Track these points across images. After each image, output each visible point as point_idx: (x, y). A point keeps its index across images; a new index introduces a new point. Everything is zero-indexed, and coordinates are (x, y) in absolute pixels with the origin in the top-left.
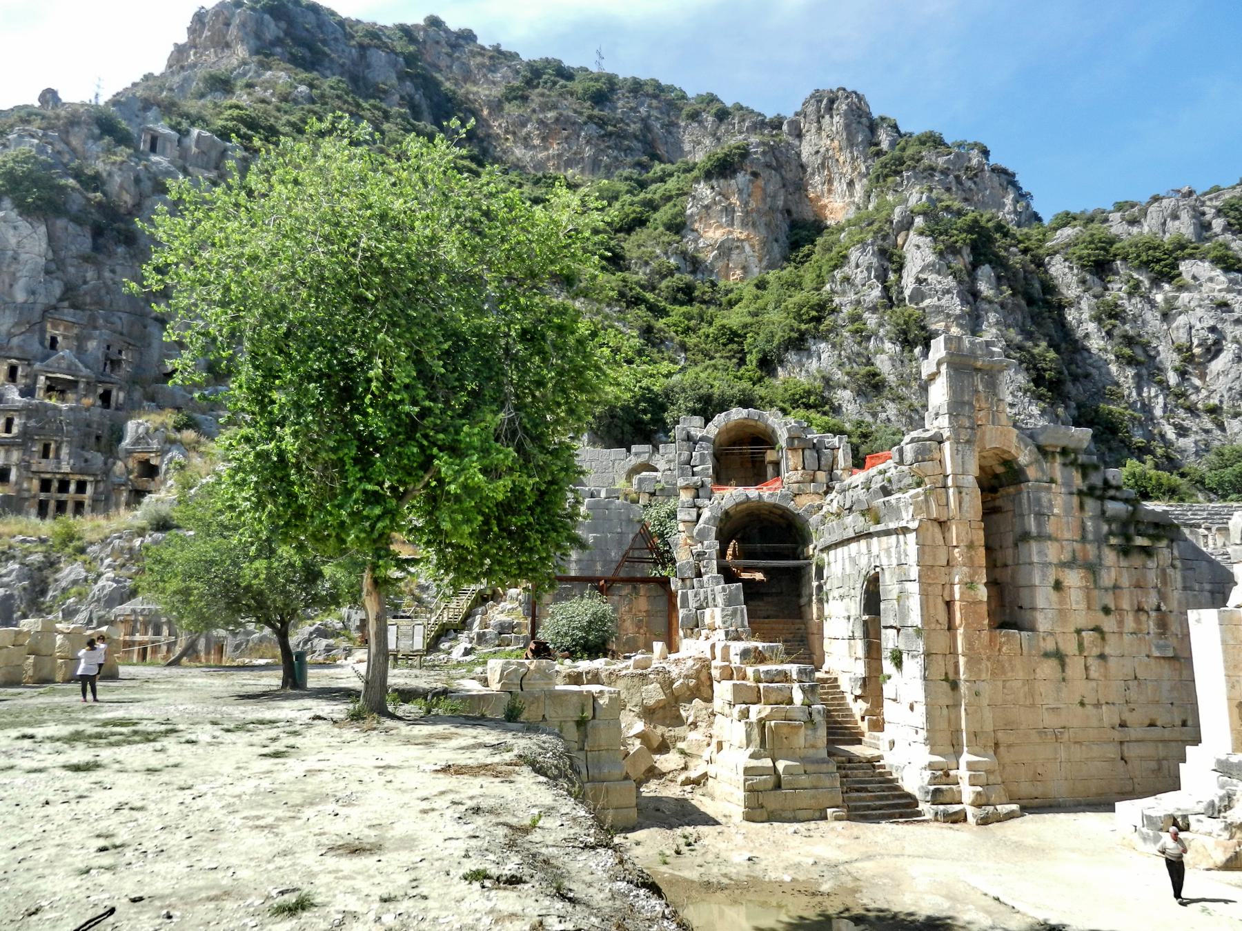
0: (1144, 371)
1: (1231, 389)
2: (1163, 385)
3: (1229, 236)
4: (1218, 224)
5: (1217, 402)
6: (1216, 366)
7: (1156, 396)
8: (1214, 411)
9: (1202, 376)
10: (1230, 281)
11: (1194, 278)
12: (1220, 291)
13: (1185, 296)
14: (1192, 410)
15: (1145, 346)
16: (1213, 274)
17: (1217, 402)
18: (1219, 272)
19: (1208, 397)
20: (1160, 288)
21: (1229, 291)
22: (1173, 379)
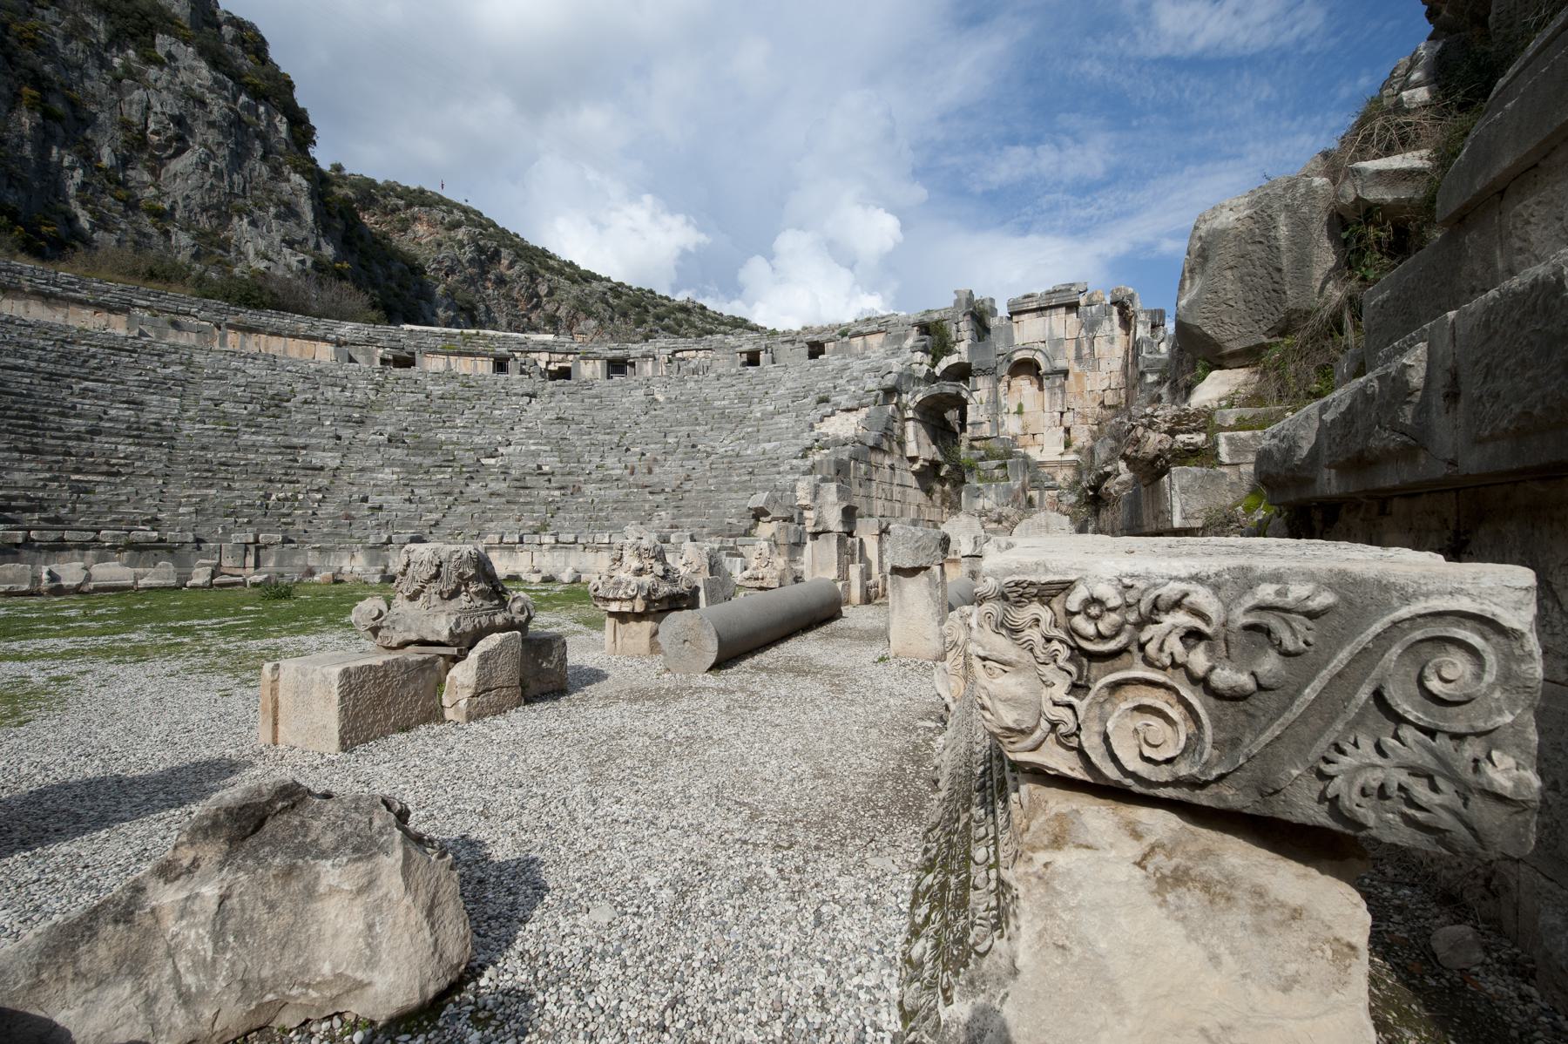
0: (59, 130)
1: (188, 197)
2: (88, 158)
3: (238, 50)
4: (228, 31)
5: (166, 206)
6: (177, 165)
7: (72, 168)
8: (160, 216)
9: (154, 172)
10: (216, 80)
11: (170, 56)
12: (200, 86)
13: (153, 72)
14: (131, 205)
15: (73, 104)
16: (195, 63)
17: (166, 206)
18: (203, 64)
19: (158, 198)
20: (122, 49)
21: (211, 91)
22: (107, 158)
